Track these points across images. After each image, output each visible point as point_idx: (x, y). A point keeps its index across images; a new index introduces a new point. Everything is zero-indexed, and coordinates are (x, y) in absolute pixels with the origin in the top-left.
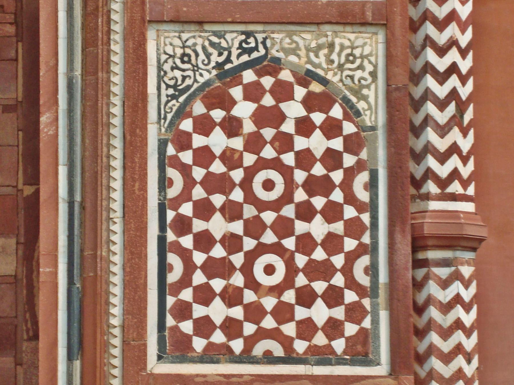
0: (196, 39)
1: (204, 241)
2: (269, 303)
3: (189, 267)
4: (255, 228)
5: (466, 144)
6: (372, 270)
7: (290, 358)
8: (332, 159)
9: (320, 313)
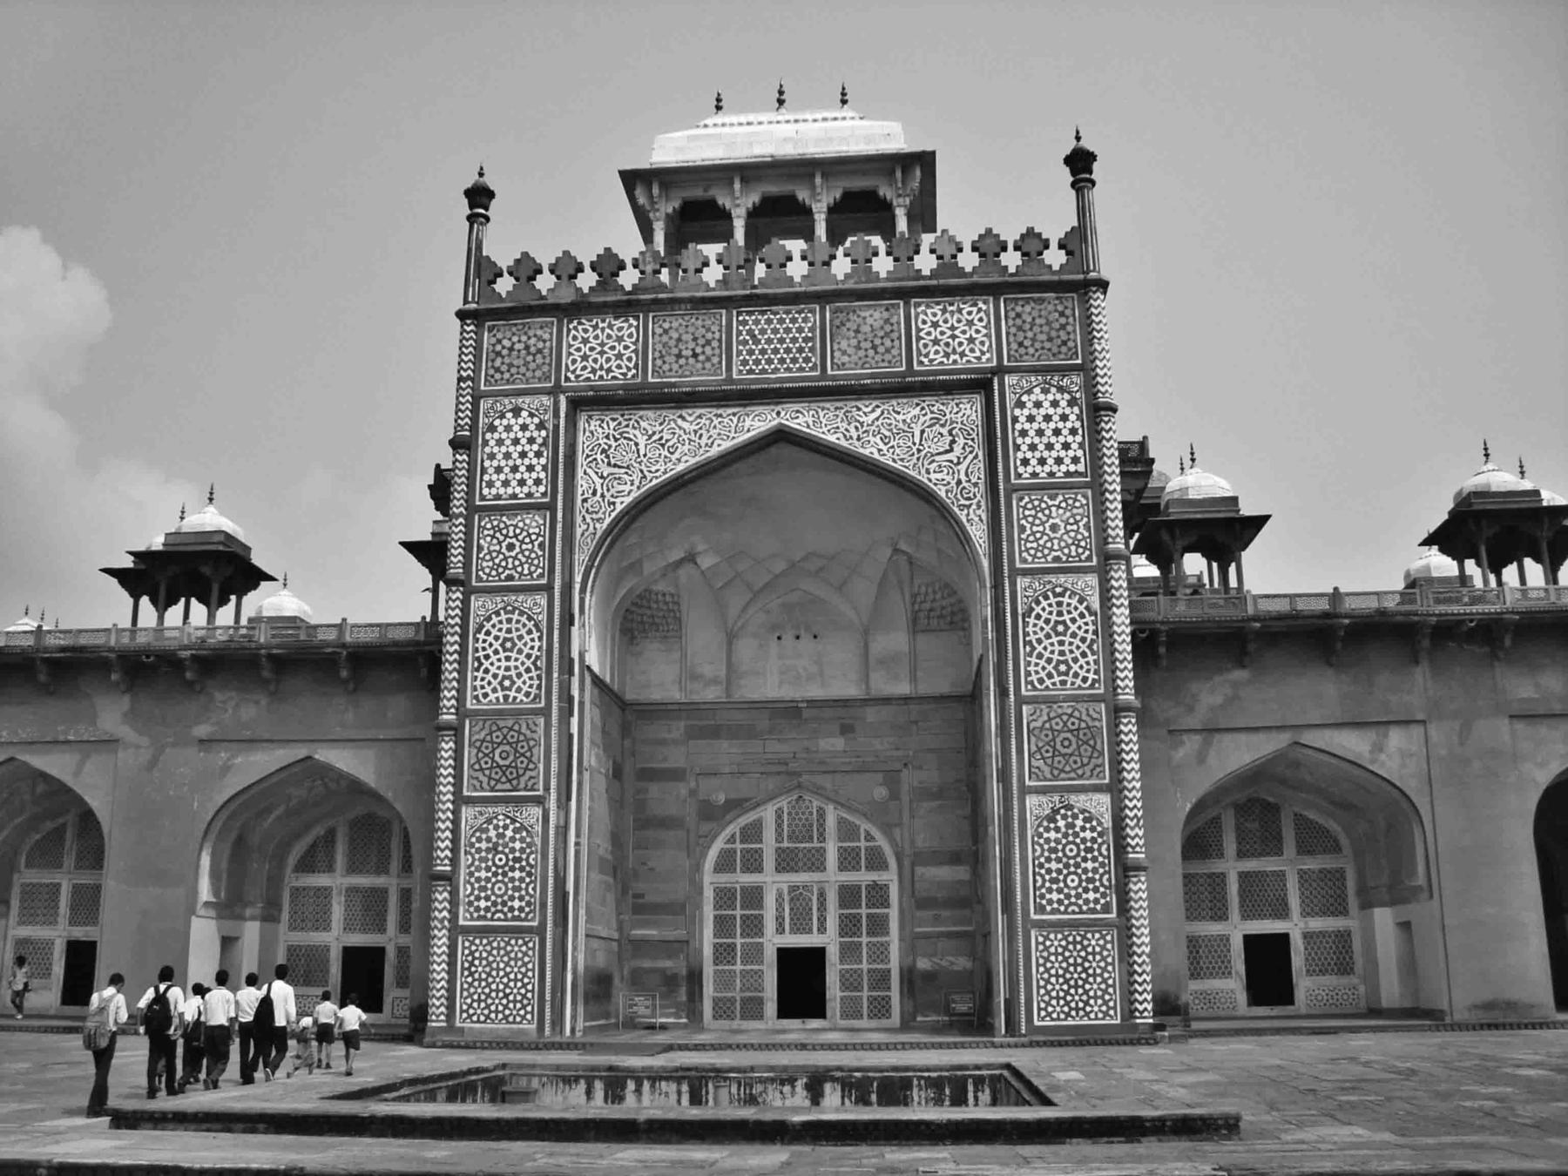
0: (1044, 799)
1: (1049, 871)
2: (1073, 893)
3: (1044, 881)
4: (1067, 866)
5: (1141, 833)
6: (1109, 880)
7: (1081, 912)
8: (1094, 840)
9: (1091, 895)
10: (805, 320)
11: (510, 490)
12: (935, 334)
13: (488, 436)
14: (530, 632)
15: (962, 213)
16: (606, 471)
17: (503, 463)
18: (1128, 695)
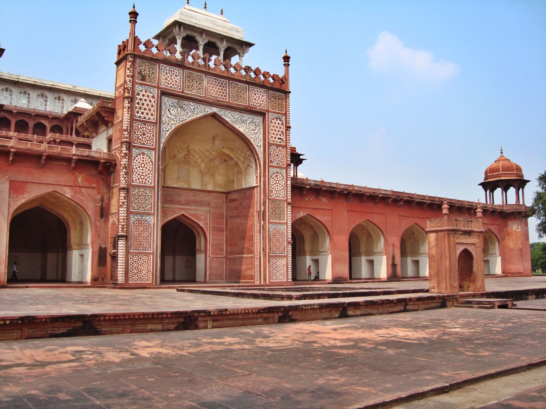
10: (225, 84)
11: (144, 116)
12: (255, 97)
13: (137, 96)
14: (149, 162)
15: (248, 60)
16: (170, 116)
17: (142, 106)
18: (289, 201)
